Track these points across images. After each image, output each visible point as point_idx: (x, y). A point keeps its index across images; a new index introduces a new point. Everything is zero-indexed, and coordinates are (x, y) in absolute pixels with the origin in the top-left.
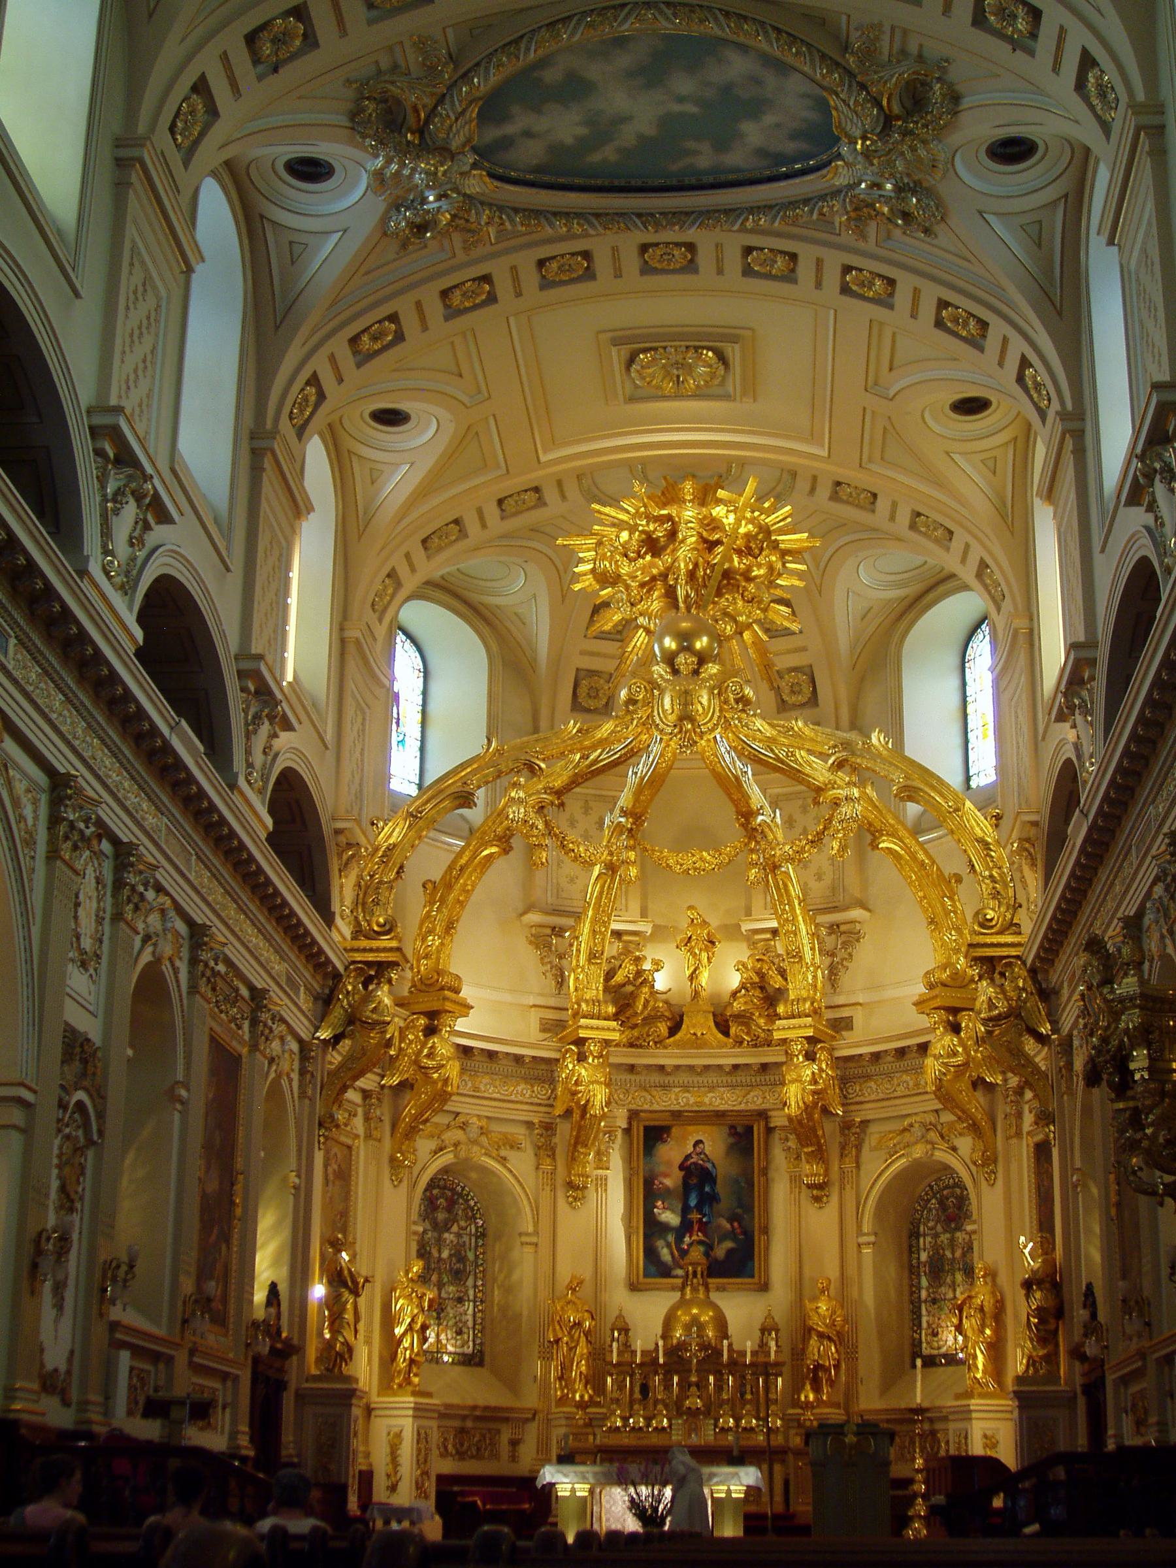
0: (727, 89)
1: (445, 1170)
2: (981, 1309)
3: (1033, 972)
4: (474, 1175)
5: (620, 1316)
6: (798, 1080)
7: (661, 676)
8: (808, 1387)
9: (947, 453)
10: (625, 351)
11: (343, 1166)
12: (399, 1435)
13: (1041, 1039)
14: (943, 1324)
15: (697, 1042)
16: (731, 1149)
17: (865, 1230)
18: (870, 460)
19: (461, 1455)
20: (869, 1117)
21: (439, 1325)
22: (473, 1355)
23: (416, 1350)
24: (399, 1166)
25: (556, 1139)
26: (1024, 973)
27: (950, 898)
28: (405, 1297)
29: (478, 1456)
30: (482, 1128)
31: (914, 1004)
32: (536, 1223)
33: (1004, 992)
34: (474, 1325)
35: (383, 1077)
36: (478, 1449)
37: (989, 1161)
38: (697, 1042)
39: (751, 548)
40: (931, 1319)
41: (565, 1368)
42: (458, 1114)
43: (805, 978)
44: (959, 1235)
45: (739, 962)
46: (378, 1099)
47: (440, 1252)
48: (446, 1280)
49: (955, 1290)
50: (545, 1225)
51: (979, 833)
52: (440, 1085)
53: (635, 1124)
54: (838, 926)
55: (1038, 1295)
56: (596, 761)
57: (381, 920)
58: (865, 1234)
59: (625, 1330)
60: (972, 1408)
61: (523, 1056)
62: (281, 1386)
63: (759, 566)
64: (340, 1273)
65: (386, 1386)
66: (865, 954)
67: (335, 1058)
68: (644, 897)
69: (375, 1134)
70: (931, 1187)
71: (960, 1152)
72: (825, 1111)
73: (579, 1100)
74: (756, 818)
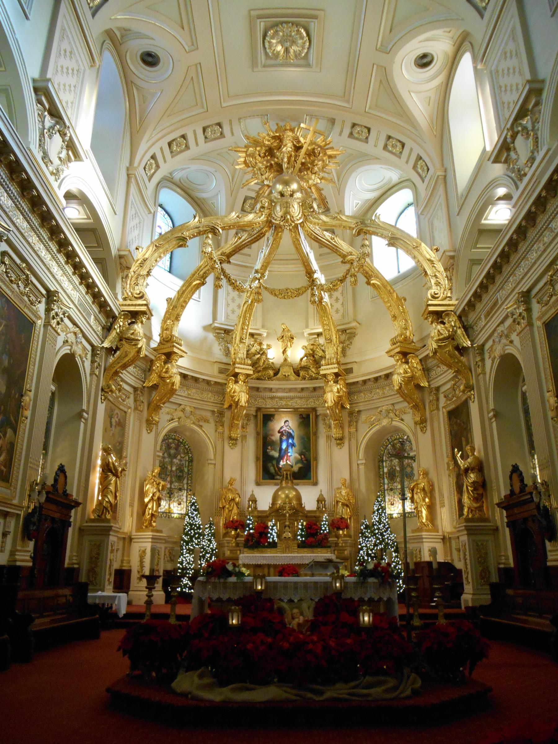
1: (174, 430)
2: (424, 489)
3: (460, 317)
4: (188, 433)
5: (253, 495)
6: (332, 391)
7: (276, 198)
9: (409, 92)
10: (261, 25)
11: (122, 421)
12: (144, 552)
14: (396, 500)
15: (286, 378)
17: (361, 458)
18: (370, 108)
20: (361, 409)
21: (170, 500)
23: (154, 509)
25: (225, 419)
26: (455, 318)
27: (402, 307)
30: (191, 412)
31: (386, 353)
32: (215, 455)
33: (446, 328)
34: (187, 500)
35: (144, 382)
38: (286, 378)
39: (315, 152)
40: (390, 498)
42: (180, 405)
45: (303, 346)
46: (142, 392)
47: (171, 467)
48: (174, 480)
51: (428, 257)
52: (170, 386)
53: (259, 413)
54: (346, 331)
56: (245, 240)
57: (138, 292)
59: (255, 501)
60: (423, 537)
61: (210, 381)
63: (319, 161)
65: (139, 528)
66: (357, 341)
68: (264, 320)
70: (388, 440)
72: (343, 407)
73: (235, 399)
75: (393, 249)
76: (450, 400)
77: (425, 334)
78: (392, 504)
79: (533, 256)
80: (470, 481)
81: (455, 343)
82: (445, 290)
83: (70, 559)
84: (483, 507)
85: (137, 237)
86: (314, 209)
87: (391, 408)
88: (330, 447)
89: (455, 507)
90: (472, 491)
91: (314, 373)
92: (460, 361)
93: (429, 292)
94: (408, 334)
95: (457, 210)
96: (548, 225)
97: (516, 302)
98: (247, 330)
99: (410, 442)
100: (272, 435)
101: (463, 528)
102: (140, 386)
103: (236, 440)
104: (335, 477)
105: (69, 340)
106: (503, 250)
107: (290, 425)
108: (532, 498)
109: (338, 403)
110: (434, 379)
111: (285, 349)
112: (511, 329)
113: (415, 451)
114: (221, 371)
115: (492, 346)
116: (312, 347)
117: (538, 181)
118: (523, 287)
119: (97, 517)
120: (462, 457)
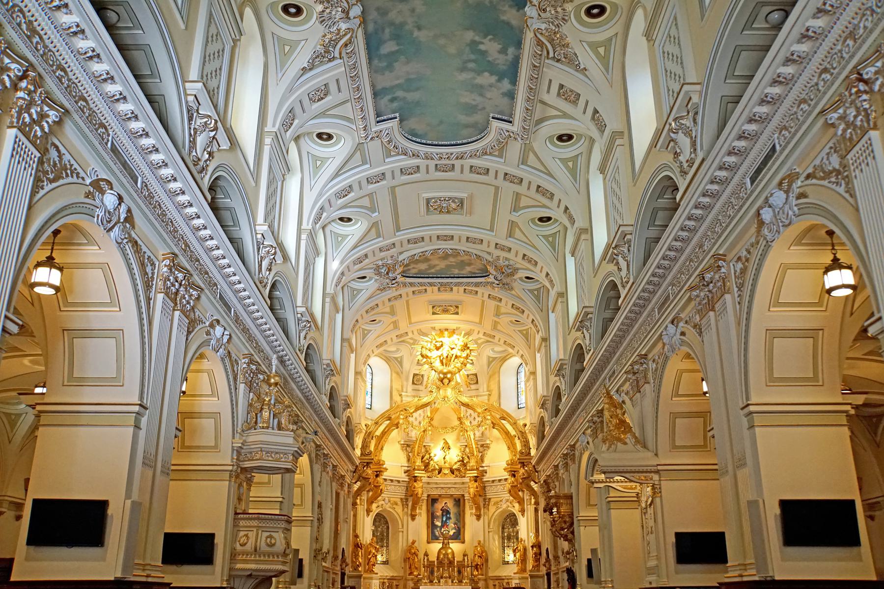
0: (462, 261)
13: (536, 483)
16: (454, 505)
17: (491, 527)
37: (523, 511)
67: (356, 487)
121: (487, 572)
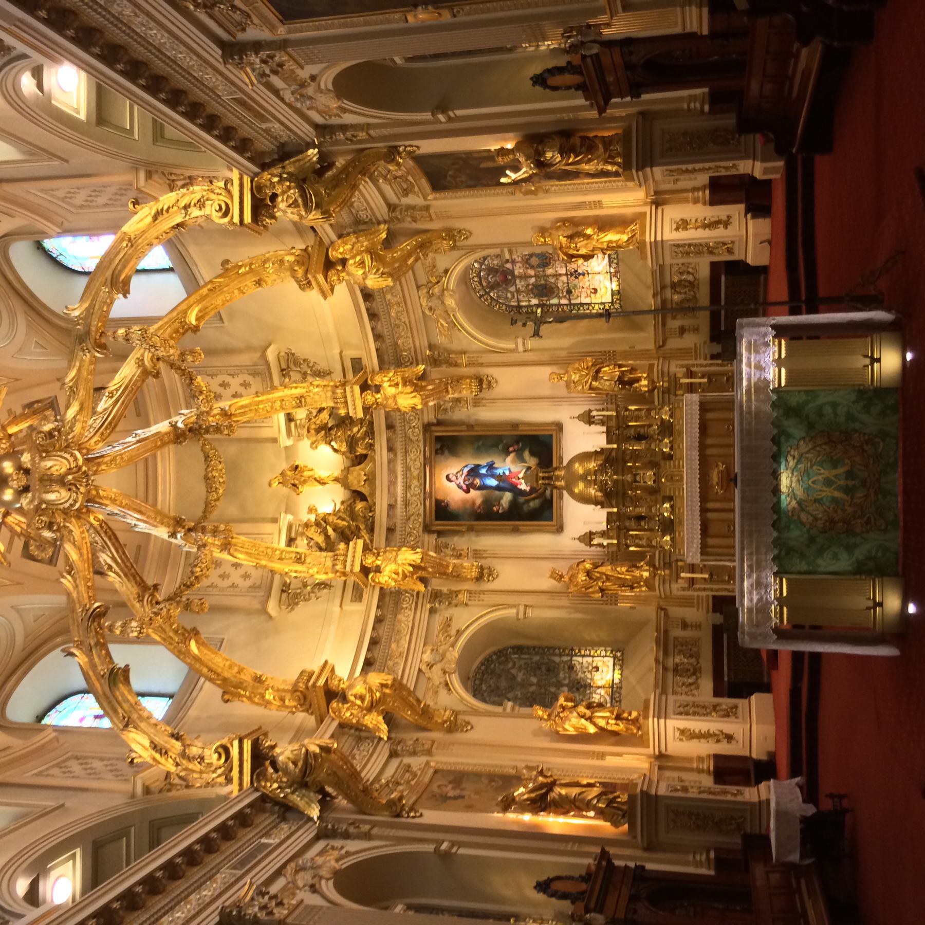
1: (465, 681)
2: (571, 237)
3: (264, 167)
5: (582, 539)
6: (394, 397)
7: (31, 501)
8: (636, 385)
11: (451, 778)
12: (683, 732)
14: (587, 284)
15: (371, 479)
17: (511, 346)
19: (696, 671)
20: (426, 344)
22: (614, 657)
23: (608, 714)
24: (456, 725)
25: (445, 590)
26: (266, 175)
27: (240, 267)
28: (564, 723)
29: (697, 656)
30: (432, 650)
31: (325, 297)
32: (510, 606)
33: (283, 193)
34: (590, 656)
35: (381, 739)
36: (691, 656)
37: (451, 234)
40: (583, 295)
41: (623, 584)
42: (420, 670)
43: (317, 393)
44: (518, 270)
45: (311, 447)
46: (399, 742)
48: (554, 680)
49: (560, 275)
50: (511, 599)
51: (150, 219)
52: (387, 691)
53: (435, 528)
54: (282, 370)
55: (549, 155)
56: (113, 558)
57: (216, 756)
58: (517, 346)
60: (653, 240)
61: (376, 616)
62: (640, 874)
64: (533, 801)
66: (303, 350)
68: (263, 520)
69: (426, 747)
70: (481, 296)
71: (448, 267)
72: (423, 377)
73: (410, 572)
74: (179, 428)
75: (137, 282)
76: (414, 187)
77: (290, 227)
78: (595, 291)
79: (157, 36)
80: (559, 159)
81: (312, 177)
82: (212, 191)
83: (698, 864)
84: (603, 137)
85: (105, 762)
86: (54, 429)
87: (425, 291)
88: (494, 400)
89: (601, 182)
90: (576, 157)
91: (361, 427)
92: (345, 168)
93: (217, 221)
94: (291, 258)
95: (57, 163)
96: (101, 6)
97: (241, 68)
98: (282, 552)
99: (485, 258)
100: (474, 503)
101: (640, 173)
102: (387, 746)
103: (482, 568)
104: (547, 392)
105: (310, 881)
106: (143, 88)
107: (455, 472)
108: (591, 56)
109: (416, 385)
110: (374, 214)
111: (315, 479)
112: (290, 78)
113: (502, 251)
114: (358, 596)
115: (319, 112)
116: (312, 432)
117: (18, 23)
118: (212, 53)
119: (626, 819)
120: (516, 169)
121: (643, 354)
